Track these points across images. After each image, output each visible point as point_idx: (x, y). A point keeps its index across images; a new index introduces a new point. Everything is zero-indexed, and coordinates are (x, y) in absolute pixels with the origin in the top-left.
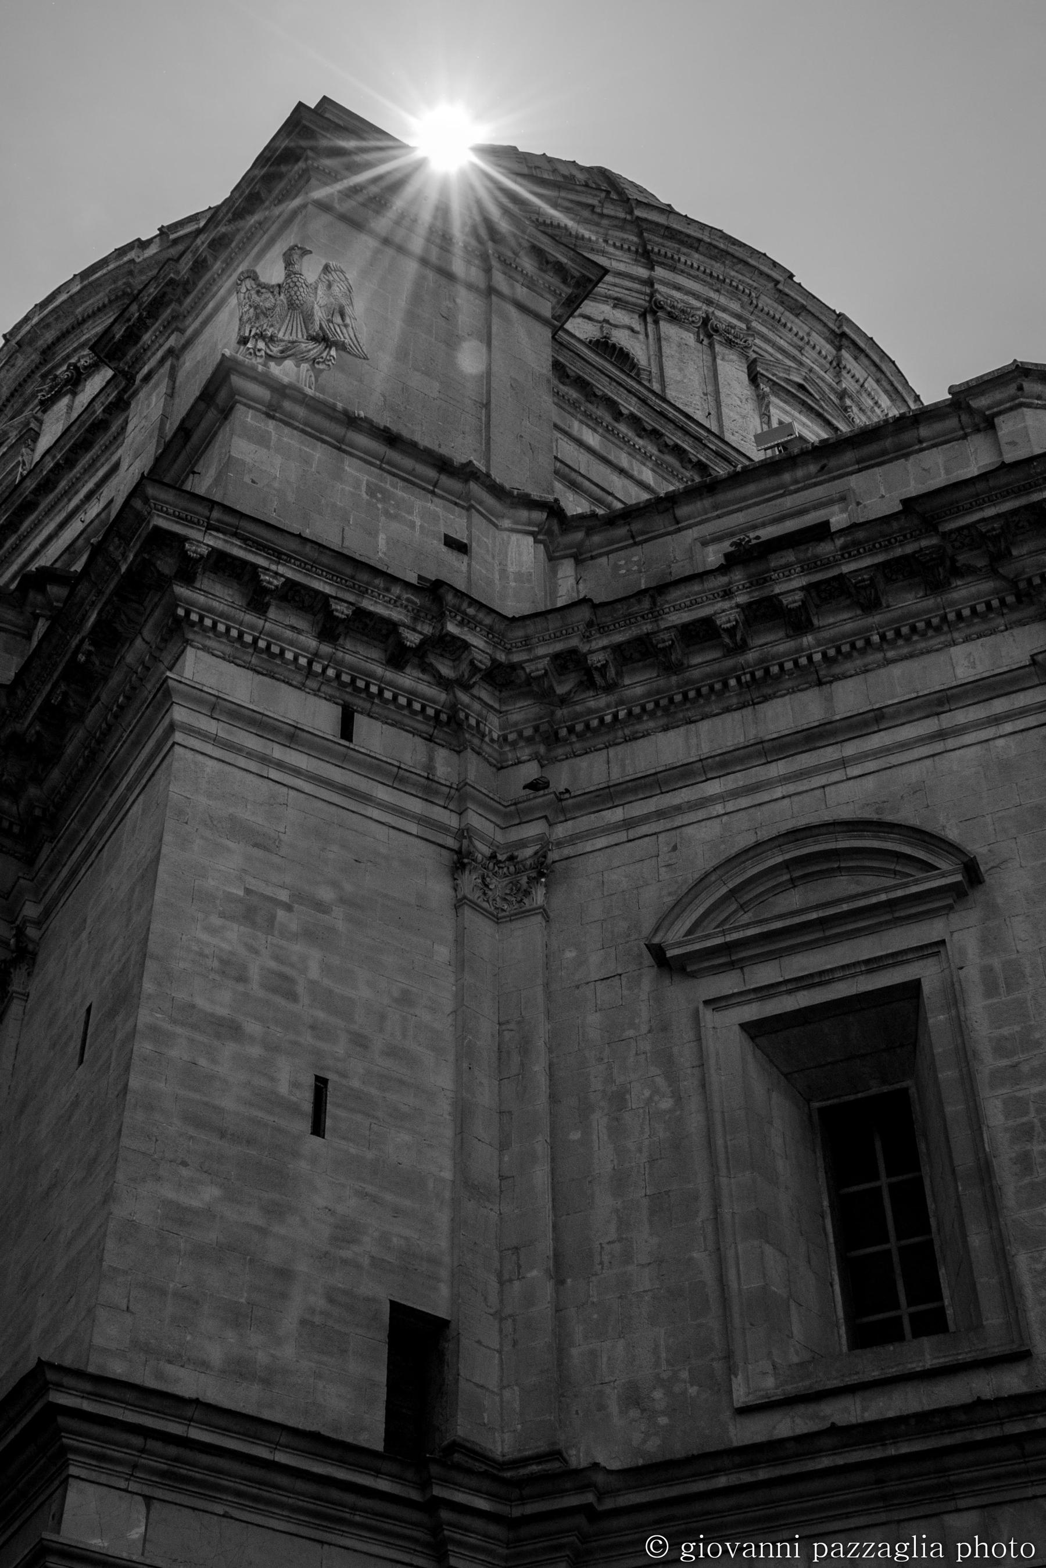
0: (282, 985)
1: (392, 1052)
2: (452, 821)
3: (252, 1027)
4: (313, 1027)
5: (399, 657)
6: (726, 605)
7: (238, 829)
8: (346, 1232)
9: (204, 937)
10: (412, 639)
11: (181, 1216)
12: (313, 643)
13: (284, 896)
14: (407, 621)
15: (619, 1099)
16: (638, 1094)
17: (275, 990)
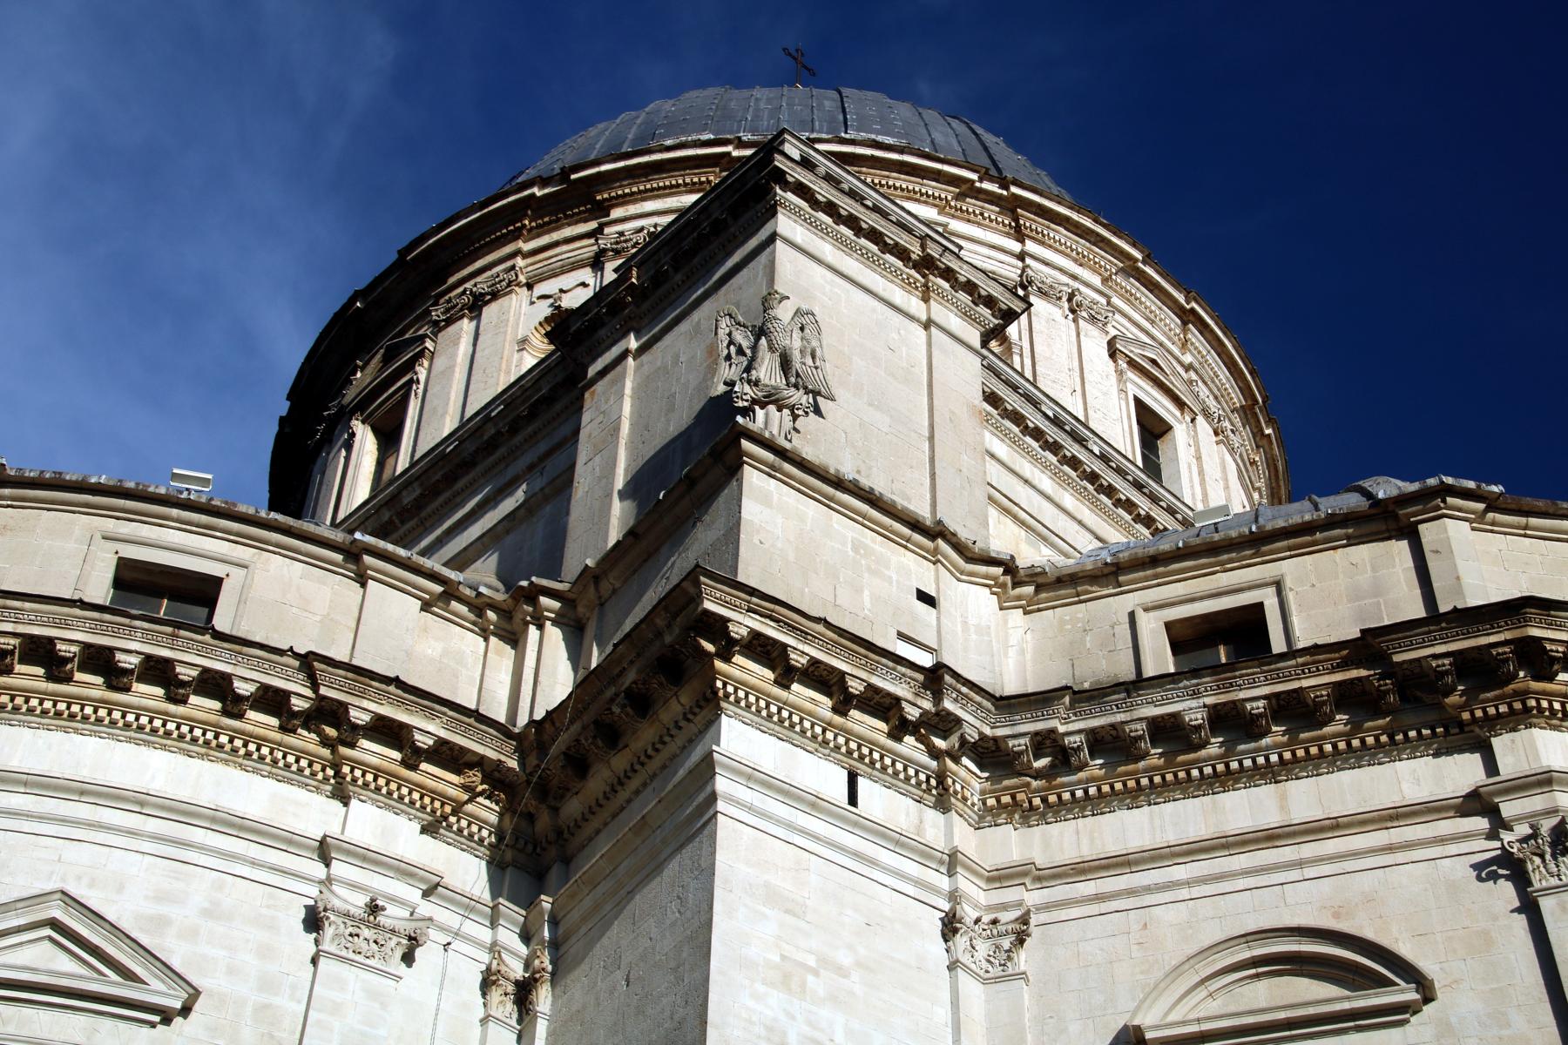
2: (944, 883)
5: (900, 728)
6: (1194, 703)
7: (772, 896)
9: (751, 1003)
10: (912, 713)
12: (829, 715)
13: (811, 961)
14: (910, 697)
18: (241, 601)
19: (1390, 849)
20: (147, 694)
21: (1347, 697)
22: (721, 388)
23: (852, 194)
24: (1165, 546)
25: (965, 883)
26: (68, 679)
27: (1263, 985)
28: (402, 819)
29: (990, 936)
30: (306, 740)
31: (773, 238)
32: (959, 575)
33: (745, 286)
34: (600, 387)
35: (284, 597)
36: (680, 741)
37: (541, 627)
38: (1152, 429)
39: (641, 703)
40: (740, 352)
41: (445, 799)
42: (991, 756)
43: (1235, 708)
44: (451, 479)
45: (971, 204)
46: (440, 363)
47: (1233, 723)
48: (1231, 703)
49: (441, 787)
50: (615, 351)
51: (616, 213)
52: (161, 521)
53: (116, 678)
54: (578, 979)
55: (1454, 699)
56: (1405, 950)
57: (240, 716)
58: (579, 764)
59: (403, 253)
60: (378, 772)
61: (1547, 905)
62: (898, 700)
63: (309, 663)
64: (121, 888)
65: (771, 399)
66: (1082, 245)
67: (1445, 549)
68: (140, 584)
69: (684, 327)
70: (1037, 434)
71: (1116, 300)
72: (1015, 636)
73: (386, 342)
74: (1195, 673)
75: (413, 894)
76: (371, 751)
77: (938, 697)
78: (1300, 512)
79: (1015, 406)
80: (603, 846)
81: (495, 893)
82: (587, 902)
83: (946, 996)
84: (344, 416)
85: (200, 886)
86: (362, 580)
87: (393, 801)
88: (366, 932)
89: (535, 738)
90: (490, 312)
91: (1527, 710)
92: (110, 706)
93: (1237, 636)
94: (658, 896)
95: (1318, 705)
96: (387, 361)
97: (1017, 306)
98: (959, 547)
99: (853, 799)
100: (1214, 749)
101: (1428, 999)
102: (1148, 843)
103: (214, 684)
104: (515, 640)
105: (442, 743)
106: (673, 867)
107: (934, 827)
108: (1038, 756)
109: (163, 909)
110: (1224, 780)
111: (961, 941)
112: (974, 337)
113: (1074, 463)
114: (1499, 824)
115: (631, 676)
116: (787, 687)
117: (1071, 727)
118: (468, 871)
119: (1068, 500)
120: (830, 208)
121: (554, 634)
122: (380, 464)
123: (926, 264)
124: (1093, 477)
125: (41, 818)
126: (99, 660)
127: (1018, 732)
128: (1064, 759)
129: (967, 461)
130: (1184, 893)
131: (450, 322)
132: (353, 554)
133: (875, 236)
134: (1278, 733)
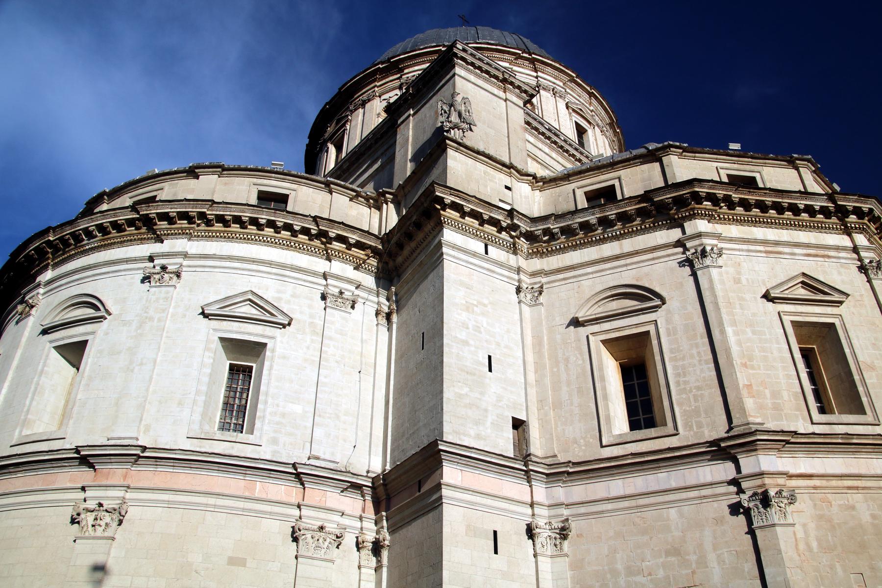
0: (477, 329)
1: (507, 347)
2: (516, 277)
3: (471, 342)
4: (486, 341)
5: (501, 230)
7: (462, 284)
8: (500, 398)
9: (457, 316)
10: (504, 224)
11: (460, 396)
12: (478, 226)
13: (475, 303)
15: (567, 360)
16: (572, 359)
17: (476, 331)
18: (295, 201)
19: (653, 259)
20: (269, 231)
21: (640, 212)
22: (440, 124)
23: (479, 59)
24: (584, 168)
25: (523, 277)
26: (246, 228)
27: (615, 303)
28: (348, 266)
29: (531, 292)
30: (317, 243)
31: (454, 75)
32: (519, 180)
33: (446, 91)
34: (402, 127)
35: (308, 199)
36: (431, 237)
37: (387, 204)
38: (581, 131)
39: (418, 226)
40: (445, 112)
41: (360, 259)
42: (530, 237)
43: (606, 217)
44: (358, 159)
45: (520, 61)
46: (353, 123)
47: (605, 222)
48: (607, 215)
49: (359, 255)
50: (406, 115)
51: (406, 71)
52: (270, 178)
53: (260, 227)
54: (404, 312)
55: (673, 212)
56: (657, 289)
57: (296, 236)
58: (400, 246)
59: (340, 89)
60: (339, 252)
61: (699, 273)
62: (499, 221)
63: (315, 219)
64: (267, 290)
65: (456, 127)
66: (556, 73)
67: (670, 165)
68: (265, 198)
69: (427, 105)
70: (543, 134)
71: (568, 90)
72: (537, 199)
73: (336, 118)
74: (593, 207)
75: (353, 288)
76: (336, 245)
77: (512, 219)
78: (626, 155)
79: (536, 126)
80: (410, 271)
81: (378, 286)
82: (406, 288)
83: (518, 311)
84: (324, 144)
85: (289, 288)
86: (331, 192)
87: (345, 260)
88: (339, 300)
89: (385, 239)
90: (368, 106)
91: (694, 214)
92: (259, 235)
93: (607, 195)
94: (426, 286)
95: (631, 216)
96: (337, 124)
97: (534, 92)
98: (518, 171)
99: (486, 253)
100: (599, 231)
101: (664, 303)
102: (579, 261)
103: (288, 227)
104: (379, 209)
105: (358, 241)
106: (431, 276)
107: (513, 260)
108: (544, 236)
109: (280, 295)
110: (603, 241)
111: (522, 294)
112: (521, 103)
113: (555, 143)
114: (686, 249)
115: (414, 218)
116: (464, 218)
117: (554, 226)
118: (369, 281)
119: (554, 155)
120: (472, 64)
121: (391, 206)
122: (337, 157)
123: (504, 81)
124: (561, 147)
125: (243, 269)
126: (254, 222)
127: (538, 229)
128: (553, 236)
129: (520, 143)
130: (591, 276)
131: (356, 110)
132: (327, 184)
133: (487, 72)
134: (619, 225)
